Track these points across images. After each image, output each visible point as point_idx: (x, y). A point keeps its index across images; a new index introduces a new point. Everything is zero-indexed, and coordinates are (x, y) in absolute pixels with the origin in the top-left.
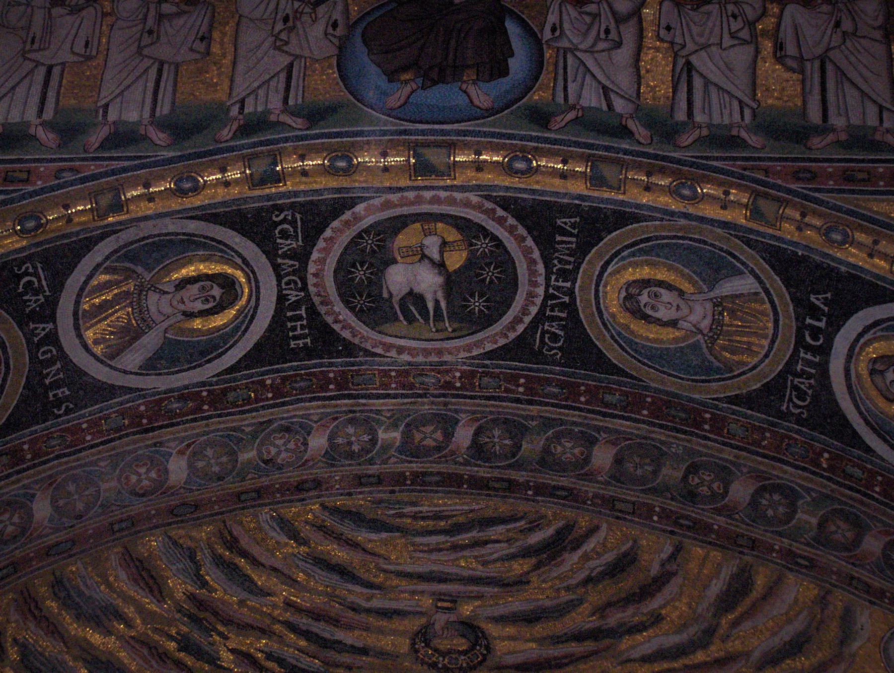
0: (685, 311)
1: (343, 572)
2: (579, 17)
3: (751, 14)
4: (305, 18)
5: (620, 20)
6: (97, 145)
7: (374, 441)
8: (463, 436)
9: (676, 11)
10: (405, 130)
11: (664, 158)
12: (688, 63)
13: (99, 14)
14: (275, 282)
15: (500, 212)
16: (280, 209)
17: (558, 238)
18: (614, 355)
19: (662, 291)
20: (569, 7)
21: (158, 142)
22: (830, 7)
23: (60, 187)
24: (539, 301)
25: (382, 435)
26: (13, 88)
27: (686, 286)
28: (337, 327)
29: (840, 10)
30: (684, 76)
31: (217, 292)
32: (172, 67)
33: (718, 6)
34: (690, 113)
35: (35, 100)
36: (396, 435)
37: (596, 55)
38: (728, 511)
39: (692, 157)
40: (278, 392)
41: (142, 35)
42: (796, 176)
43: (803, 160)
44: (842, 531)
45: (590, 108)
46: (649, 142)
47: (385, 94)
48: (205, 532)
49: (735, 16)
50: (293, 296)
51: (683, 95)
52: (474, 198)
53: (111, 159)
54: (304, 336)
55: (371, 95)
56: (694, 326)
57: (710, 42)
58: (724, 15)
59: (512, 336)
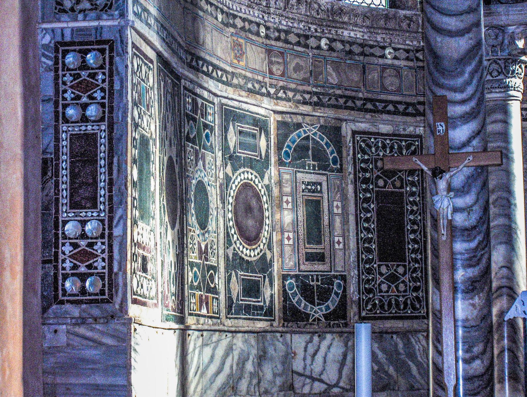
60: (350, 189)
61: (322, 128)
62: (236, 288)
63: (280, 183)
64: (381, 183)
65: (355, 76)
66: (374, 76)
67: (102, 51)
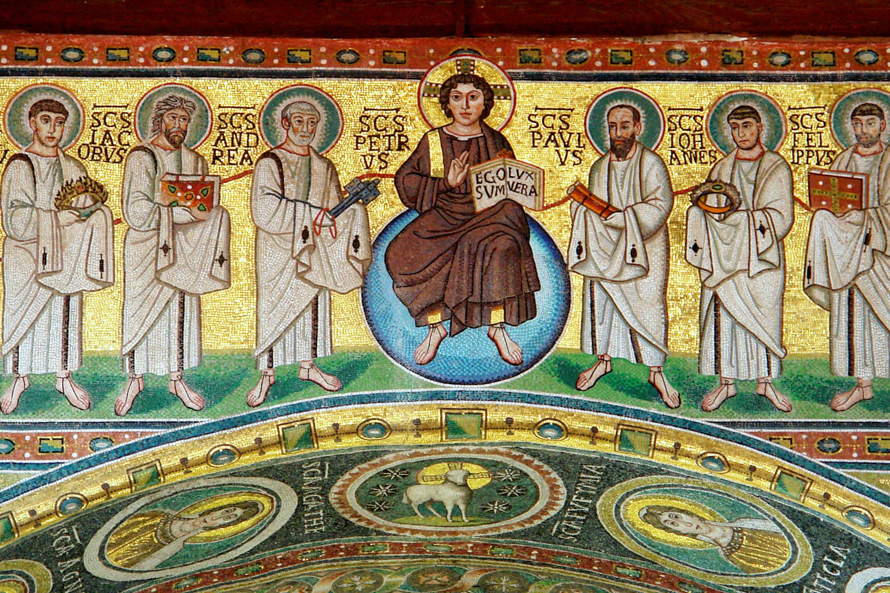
0: (704, 529)
2: (605, 234)
4: (325, 232)
5: (646, 237)
6: (128, 406)
7: (378, 583)
9: (703, 222)
10: (436, 393)
11: (692, 426)
12: (715, 297)
13: (110, 222)
14: (296, 499)
15: (526, 457)
16: (310, 462)
17: (582, 475)
18: (629, 545)
19: (683, 515)
20: (593, 214)
21: (191, 405)
22: (860, 214)
23: (99, 460)
24: (558, 508)
25: (386, 579)
26: (32, 325)
27: (706, 516)
28: (353, 520)
29: (871, 219)
30: (712, 312)
31: (239, 512)
32: (194, 301)
33: (745, 214)
34: (717, 368)
35: (57, 344)
36: (402, 580)
37: (622, 285)
39: (719, 423)
41: (157, 252)
43: (828, 425)
45: (618, 358)
46: (677, 404)
47: (413, 343)
49: (762, 230)
50: (313, 504)
51: (710, 340)
52: (501, 449)
53: (144, 425)
54: (320, 526)
55: (398, 345)
56: (714, 540)
57: (738, 268)
58: (752, 227)
59: (527, 526)
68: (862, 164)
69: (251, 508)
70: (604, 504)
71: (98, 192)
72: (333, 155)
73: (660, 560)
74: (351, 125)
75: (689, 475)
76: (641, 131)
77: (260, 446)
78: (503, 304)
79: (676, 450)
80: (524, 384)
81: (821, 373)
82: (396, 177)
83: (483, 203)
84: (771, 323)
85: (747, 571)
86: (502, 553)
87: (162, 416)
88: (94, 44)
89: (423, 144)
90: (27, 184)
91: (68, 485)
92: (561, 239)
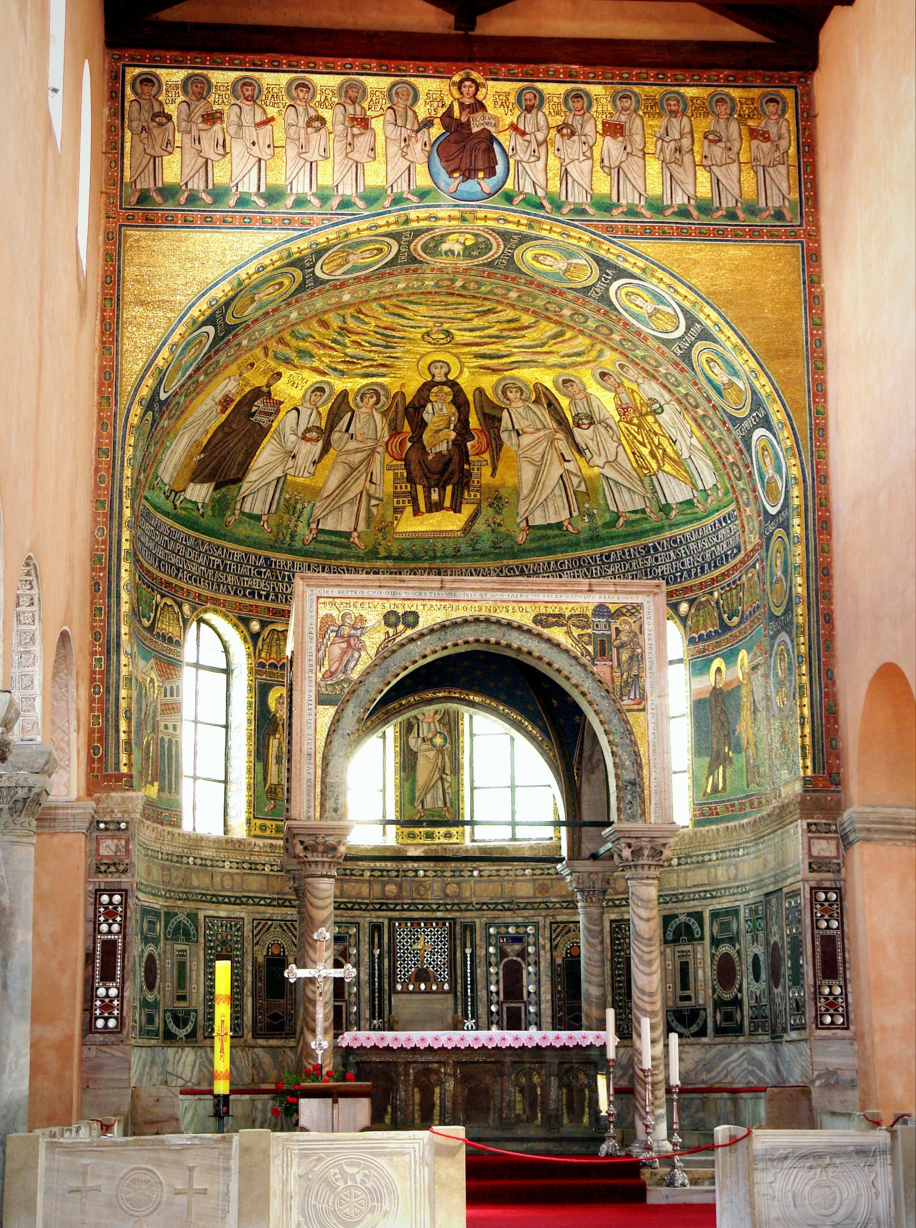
1: (399, 315)
3: (591, 143)
5: (539, 145)
8: (459, 284)
11: (557, 220)
18: (524, 270)
23: (325, 228)
35: (308, 181)
36: (432, 283)
38: (561, 316)
40: (391, 274)
42: (607, 229)
44: (605, 331)
48: (349, 312)
51: (564, 186)
55: (442, 185)
60: (202, 953)
61: (188, 915)
62: (144, 1019)
63: (165, 952)
64: (219, 949)
65: (207, 880)
66: (217, 879)
67: (121, 895)
68: (623, 118)
69: (380, 250)
70: (517, 253)
71: (323, 121)
72: (416, 109)
73: (536, 276)
74: (422, 97)
75: (554, 240)
76: (537, 102)
77: (388, 224)
78: (483, 170)
79: (550, 230)
80: (492, 202)
81: (607, 201)
82: (441, 118)
83: (475, 130)
84: (587, 180)
85: (570, 281)
86: (473, 273)
87: (349, 211)
88: (320, 61)
89: (451, 105)
90: (294, 116)
91: (313, 237)
92: (506, 145)
